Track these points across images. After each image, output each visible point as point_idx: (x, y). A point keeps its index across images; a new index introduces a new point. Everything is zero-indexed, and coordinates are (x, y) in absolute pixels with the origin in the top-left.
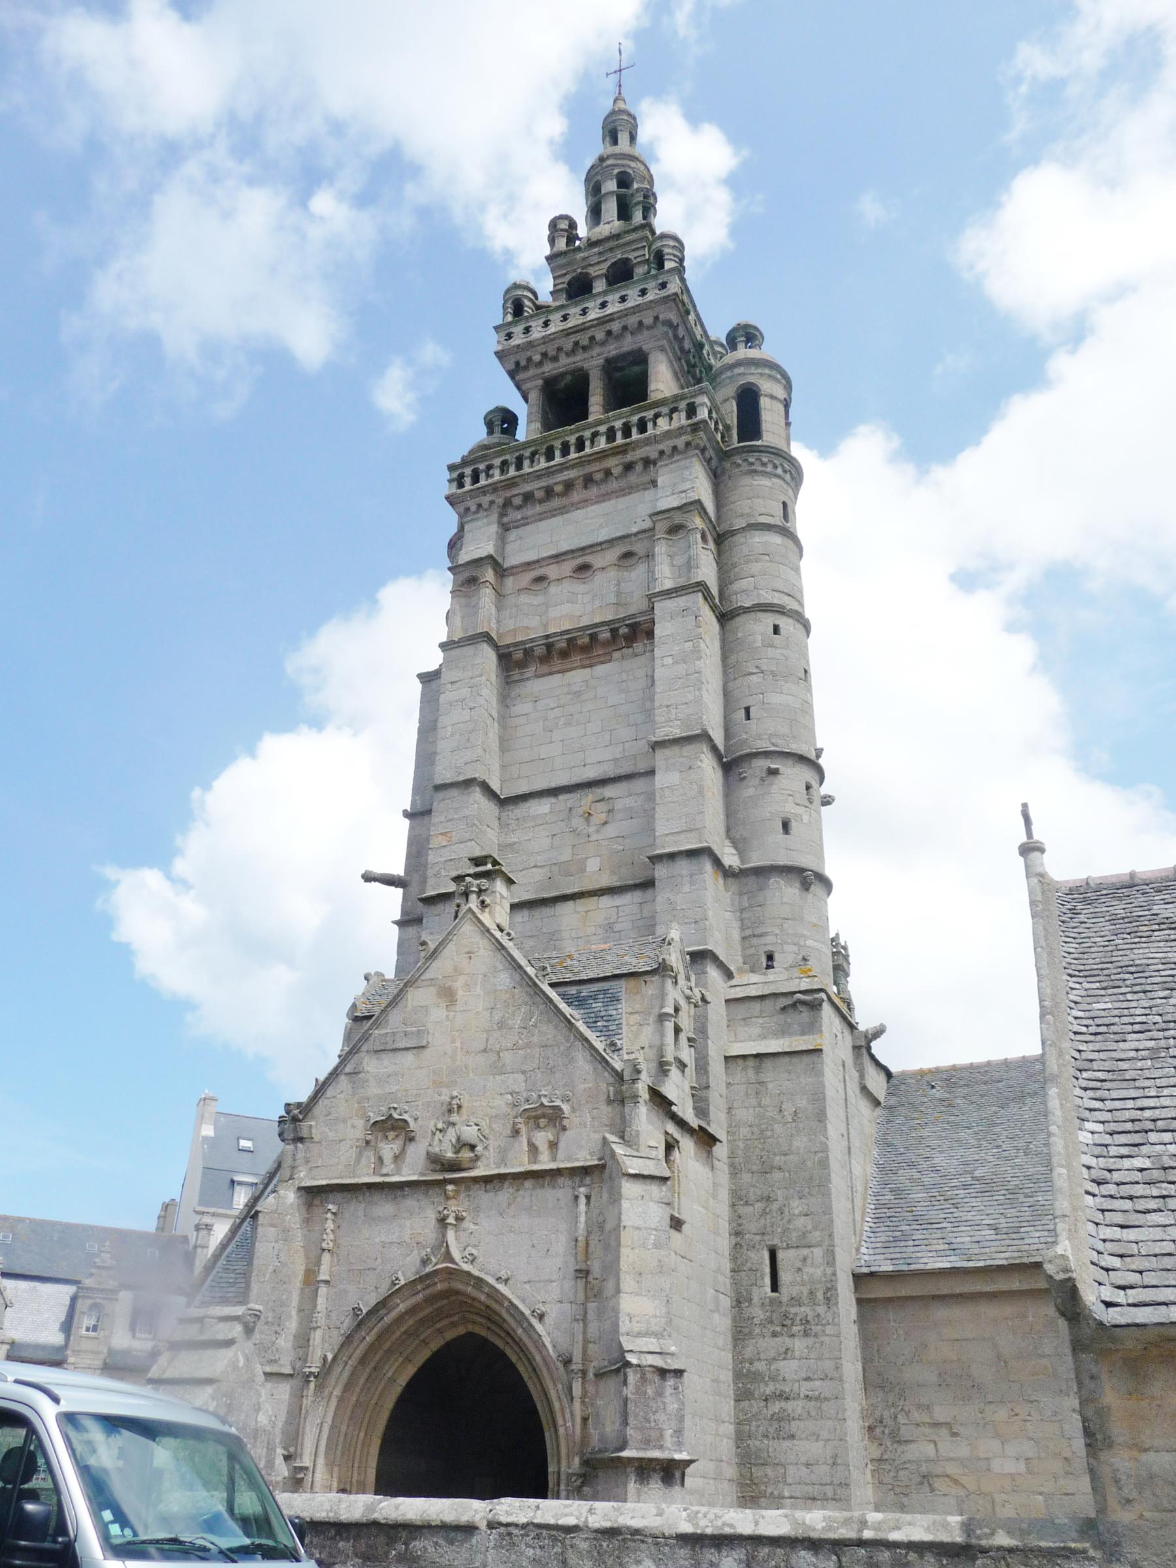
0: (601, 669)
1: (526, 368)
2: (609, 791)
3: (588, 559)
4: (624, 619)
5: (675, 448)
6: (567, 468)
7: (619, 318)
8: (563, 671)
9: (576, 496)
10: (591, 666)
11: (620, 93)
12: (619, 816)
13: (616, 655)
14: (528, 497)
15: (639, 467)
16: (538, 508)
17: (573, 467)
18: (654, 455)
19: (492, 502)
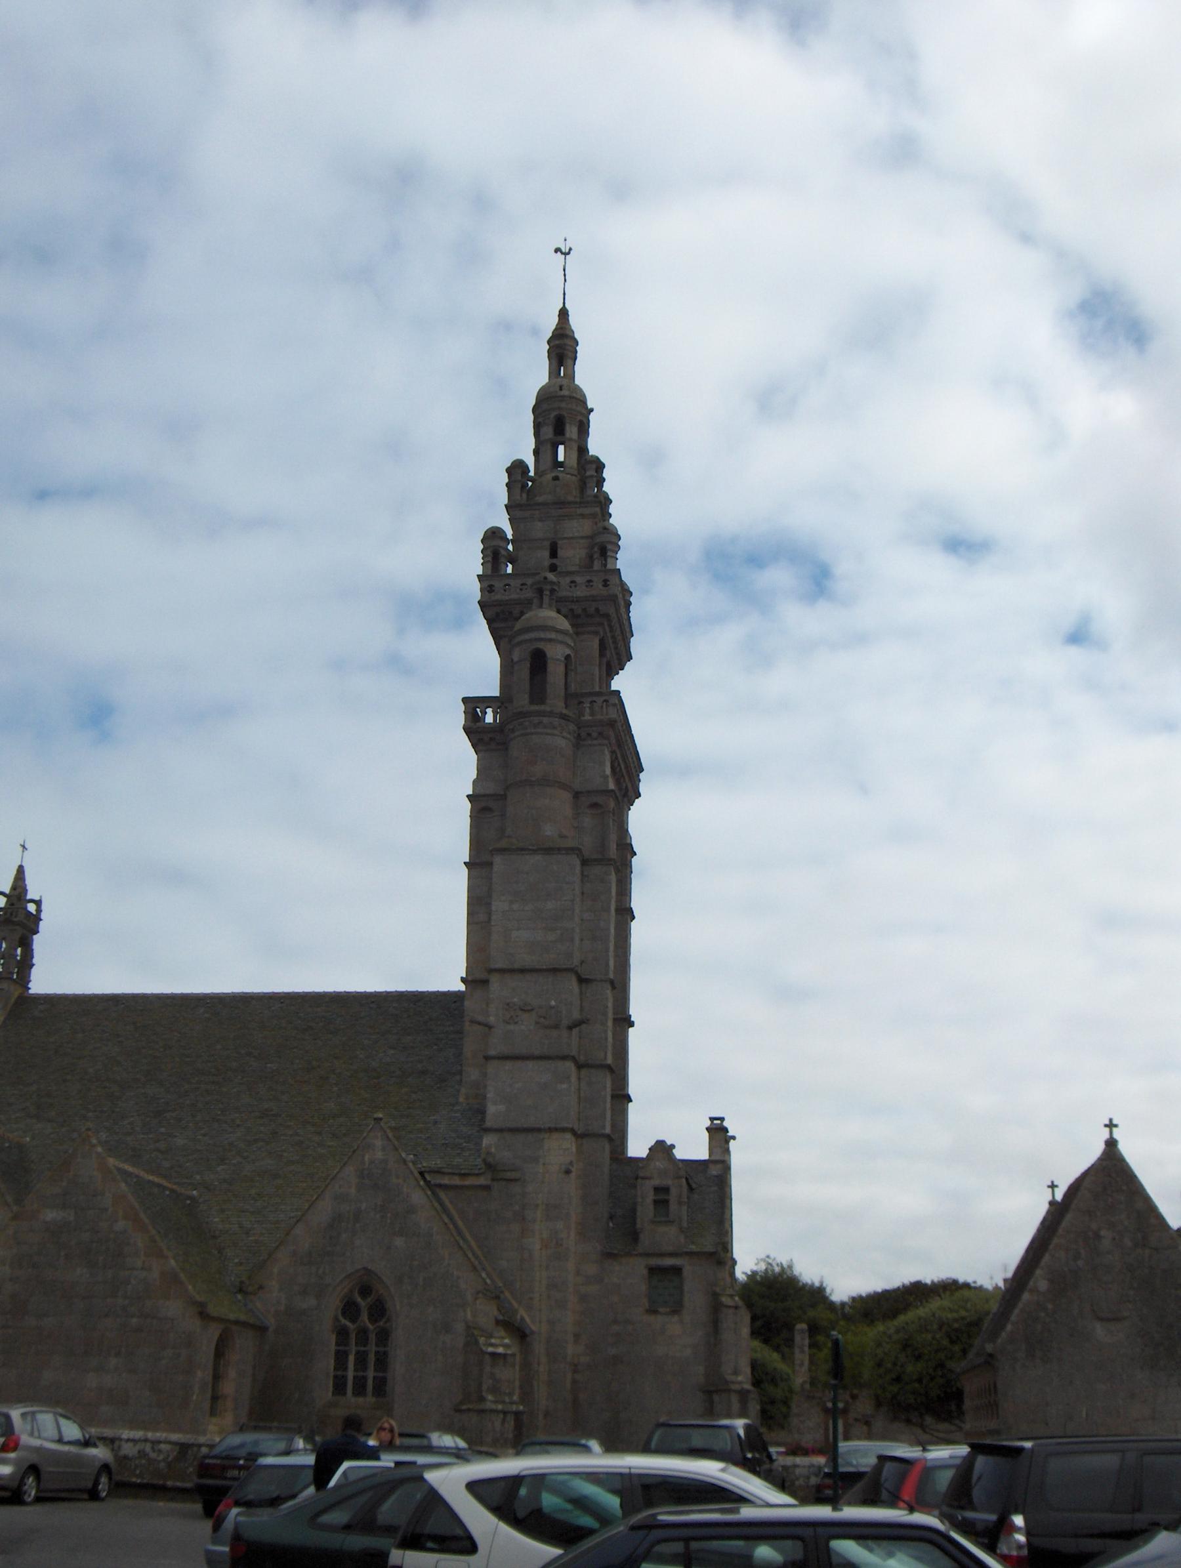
11: (564, 303)
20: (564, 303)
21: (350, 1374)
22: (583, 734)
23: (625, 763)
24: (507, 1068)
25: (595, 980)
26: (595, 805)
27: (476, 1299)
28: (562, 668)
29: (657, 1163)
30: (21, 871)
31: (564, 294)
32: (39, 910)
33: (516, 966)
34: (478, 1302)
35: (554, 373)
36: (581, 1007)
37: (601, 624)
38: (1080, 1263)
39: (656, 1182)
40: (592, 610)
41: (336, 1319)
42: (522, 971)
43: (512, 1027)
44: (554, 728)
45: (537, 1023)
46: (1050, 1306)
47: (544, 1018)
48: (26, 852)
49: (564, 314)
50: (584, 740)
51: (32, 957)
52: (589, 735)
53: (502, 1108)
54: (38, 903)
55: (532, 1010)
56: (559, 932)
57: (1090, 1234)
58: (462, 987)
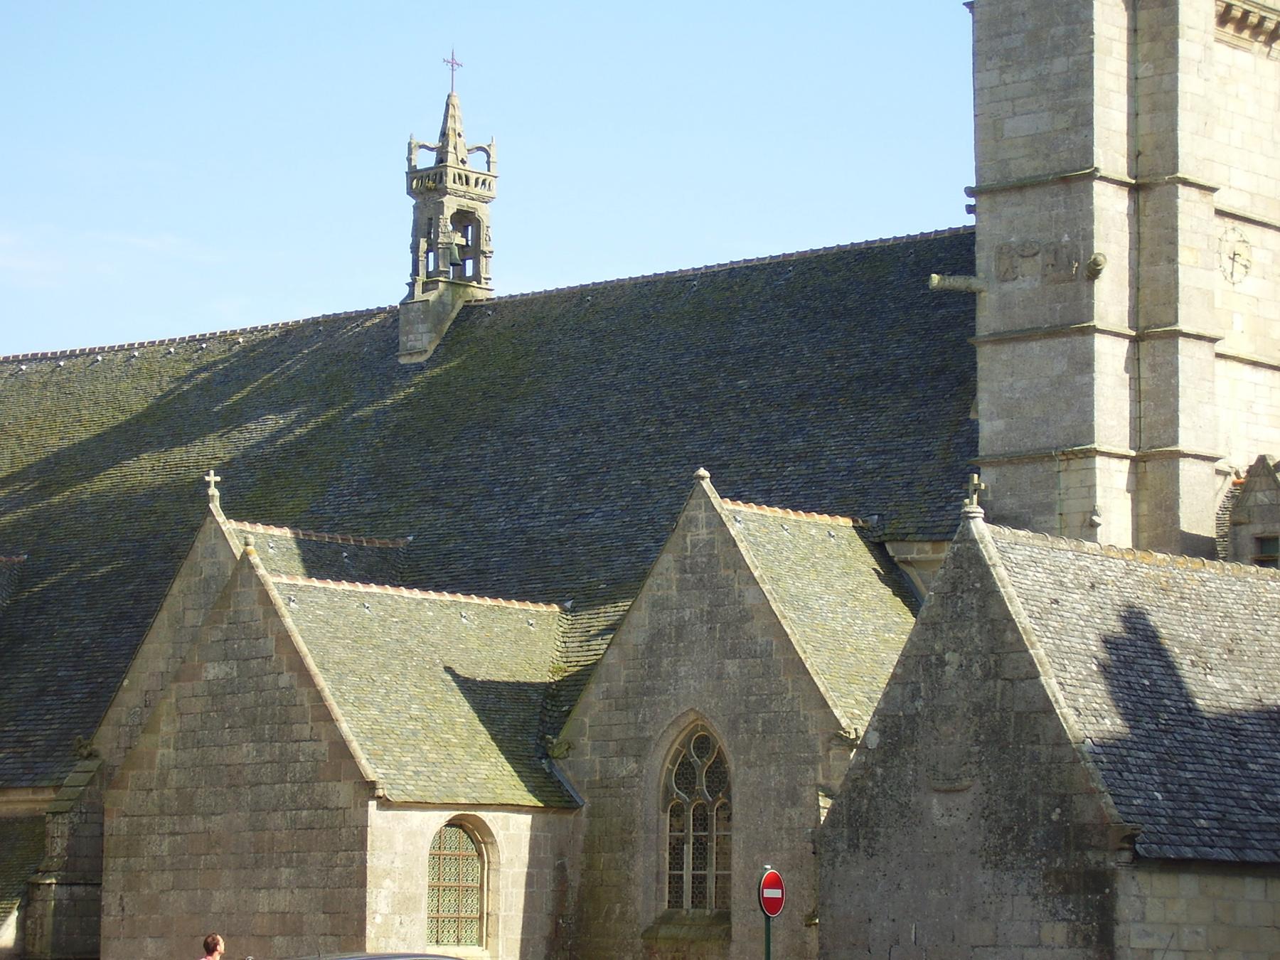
21: (687, 873)
24: (1004, 357)
27: (829, 750)
29: (1260, 495)
33: (1013, 178)
34: (831, 753)
38: (919, 704)
39: (1257, 529)
41: (668, 791)
42: (1021, 186)
43: (1007, 287)
46: (879, 771)
48: (458, 70)
53: (999, 424)
56: (1072, 111)
57: (933, 658)
58: (970, 220)
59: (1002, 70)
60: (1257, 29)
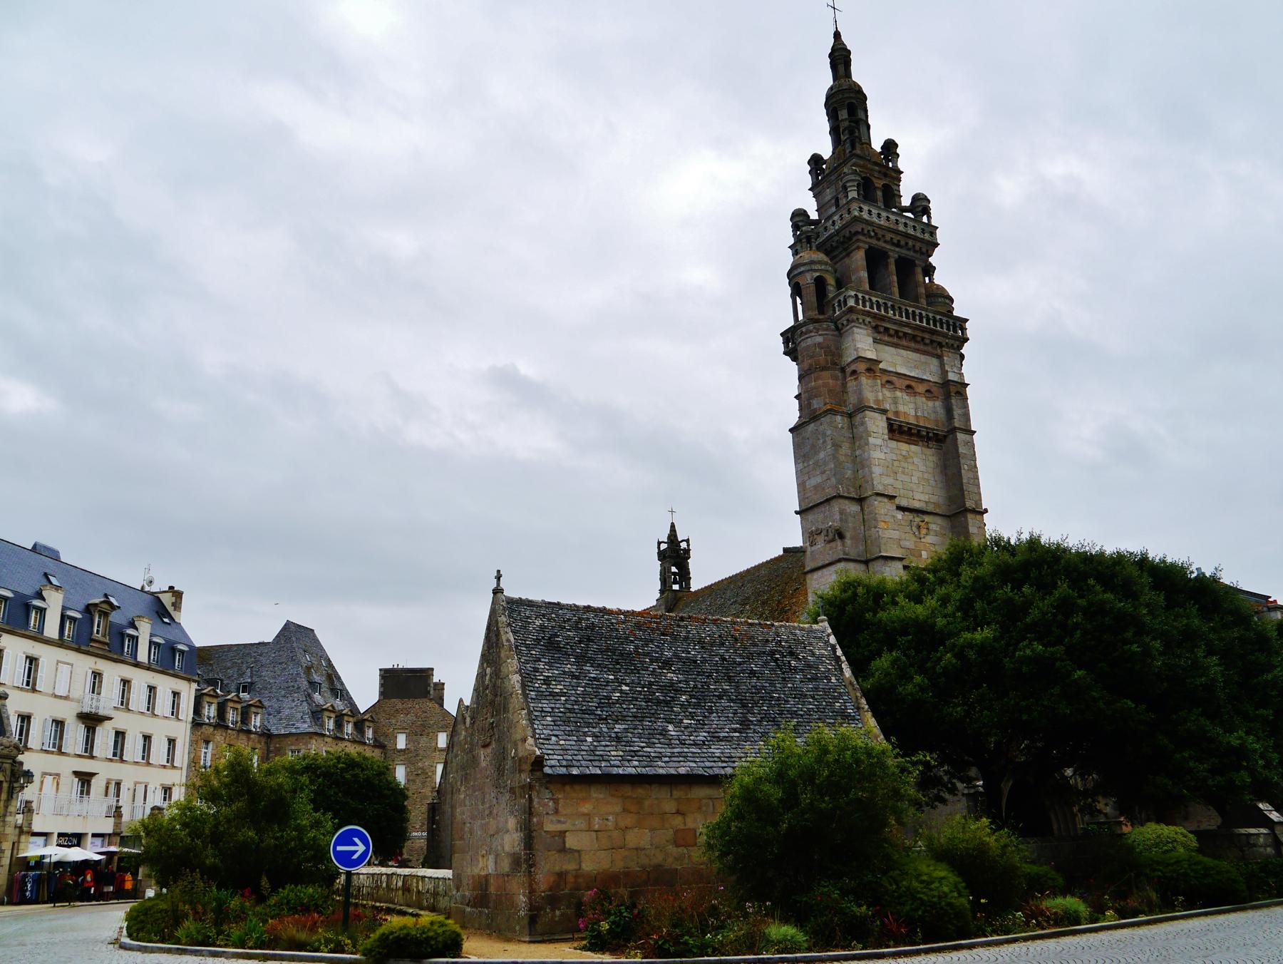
0: (913, 448)
1: (864, 235)
2: (927, 518)
3: (913, 384)
4: (934, 429)
5: (952, 345)
6: (908, 326)
7: (913, 239)
8: (898, 441)
9: (904, 343)
10: (909, 444)
11: (837, 28)
12: (932, 533)
13: (920, 443)
14: (887, 329)
15: (935, 345)
16: (886, 338)
17: (911, 328)
18: (944, 343)
19: (870, 322)
20: (837, 28)
22: (840, 326)
23: (905, 326)
24: (815, 577)
25: (867, 497)
26: (854, 372)
28: (813, 288)
30: (673, 526)
31: (836, 21)
32: (688, 545)
35: (836, 77)
36: (864, 519)
37: (858, 240)
40: (847, 235)
43: (813, 548)
44: (811, 332)
45: (825, 541)
47: (827, 536)
49: (837, 35)
50: (842, 329)
51: (689, 573)
52: (843, 324)
54: (687, 541)
55: (821, 532)
59: (803, 462)
60: (919, 435)
